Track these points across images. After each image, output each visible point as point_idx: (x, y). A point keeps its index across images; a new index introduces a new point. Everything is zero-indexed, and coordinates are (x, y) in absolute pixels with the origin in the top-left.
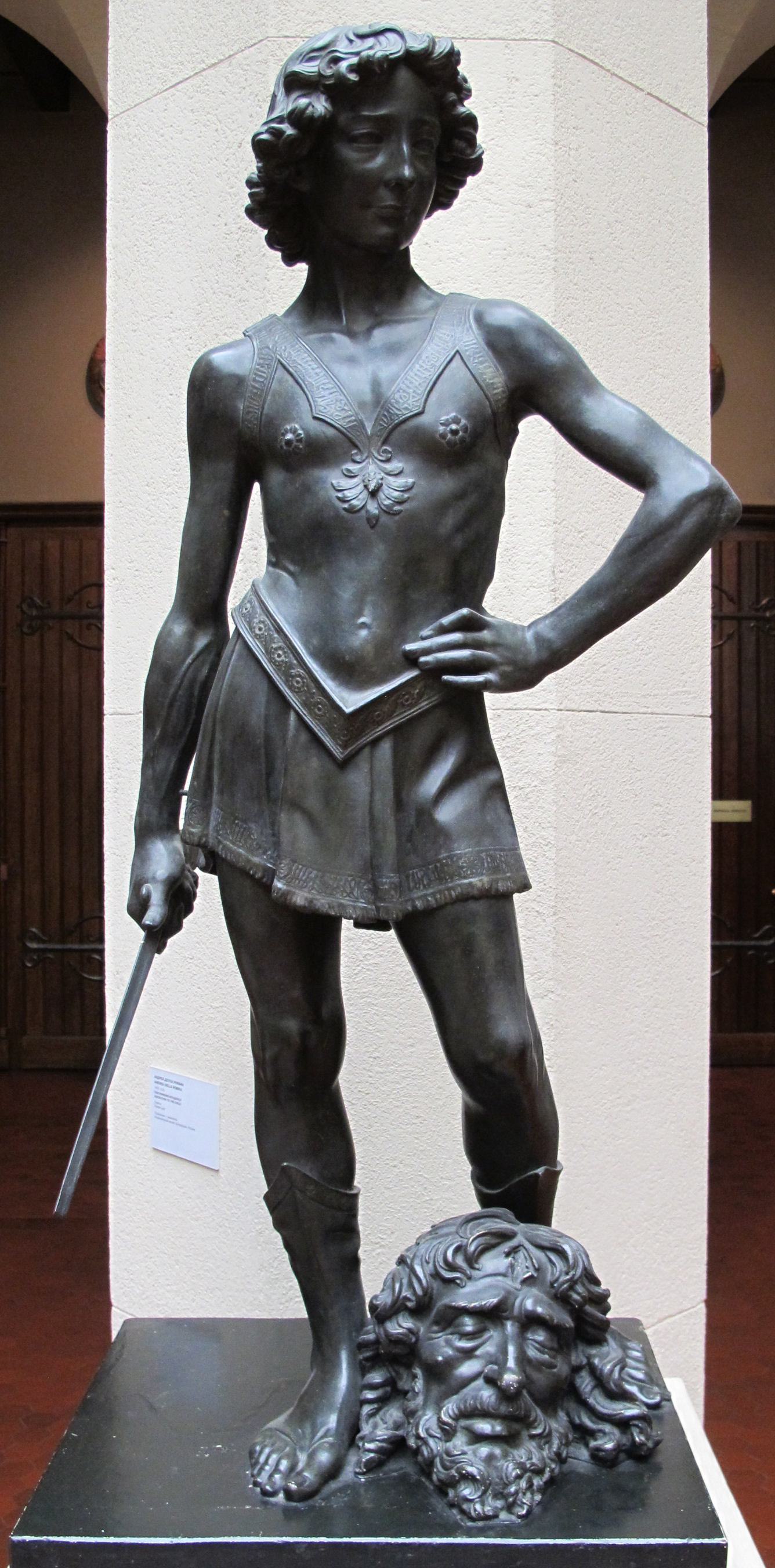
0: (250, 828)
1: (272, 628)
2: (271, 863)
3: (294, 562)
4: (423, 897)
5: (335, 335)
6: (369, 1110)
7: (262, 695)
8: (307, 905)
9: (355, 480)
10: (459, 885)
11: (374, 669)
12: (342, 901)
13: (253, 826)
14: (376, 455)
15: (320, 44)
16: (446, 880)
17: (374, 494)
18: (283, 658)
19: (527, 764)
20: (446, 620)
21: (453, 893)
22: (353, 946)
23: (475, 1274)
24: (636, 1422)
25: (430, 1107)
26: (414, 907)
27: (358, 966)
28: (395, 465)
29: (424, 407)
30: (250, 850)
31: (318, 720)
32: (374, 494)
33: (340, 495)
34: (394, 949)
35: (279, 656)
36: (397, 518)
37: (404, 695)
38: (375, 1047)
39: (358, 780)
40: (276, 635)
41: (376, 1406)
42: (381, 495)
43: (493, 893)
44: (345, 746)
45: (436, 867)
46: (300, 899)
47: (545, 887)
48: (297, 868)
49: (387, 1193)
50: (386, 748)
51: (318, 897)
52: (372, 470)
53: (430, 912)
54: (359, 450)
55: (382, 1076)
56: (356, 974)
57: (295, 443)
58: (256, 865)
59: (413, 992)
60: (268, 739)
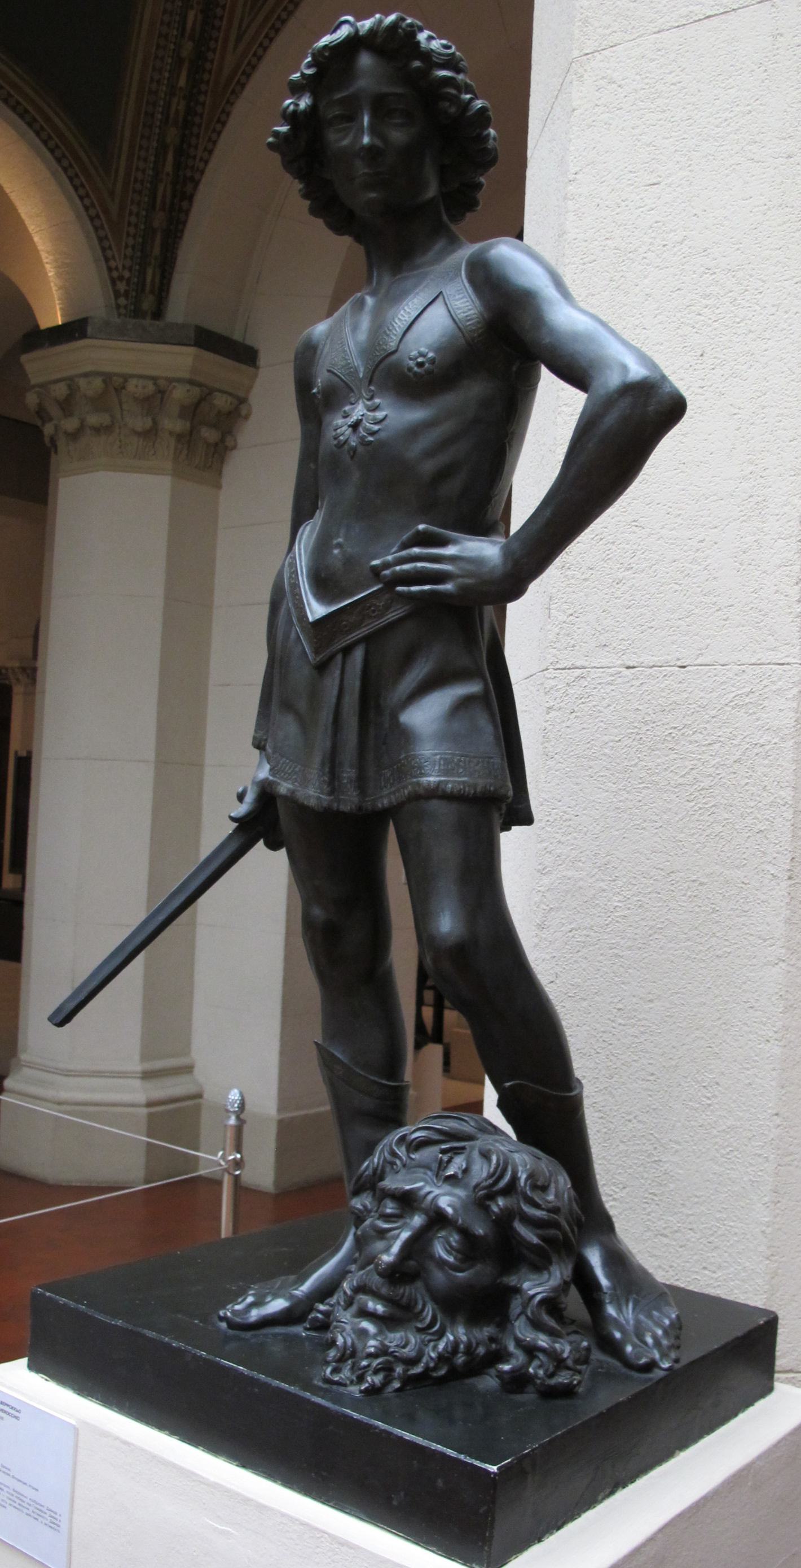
6: (611, 1061)
8: (289, 795)
19: (768, 721)
22: (605, 897)
25: (664, 1066)
27: (609, 917)
29: (398, 346)
34: (640, 903)
37: (370, 607)
38: (619, 998)
43: (440, 793)
47: (781, 849)
49: (622, 1147)
50: (359, 654)
51: (300, 789)
55: (625, 1028)
56: (607, 925)
59: (655, 947)
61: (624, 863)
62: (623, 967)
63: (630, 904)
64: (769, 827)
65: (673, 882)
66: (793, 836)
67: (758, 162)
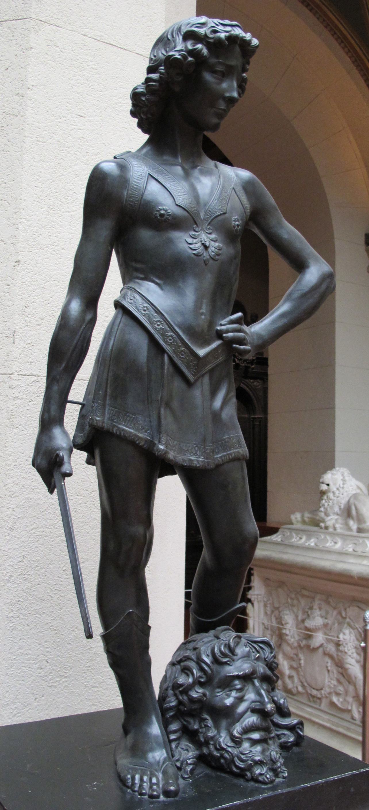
0: (137, 418)
2: (149, 437)
3: (159, 278)
6: (60, 600)
9: (197, 240)
11: (207, 337)
12: (191, 458)
13: (139, 417)
16: (228, 450)
18: (161, 326)
21: (231, 456)
22: (54, 508)
25: (91, 596)
27: (57, 519)
28: (213, 236)
30: (138, 430)
31: (181, 360)
34: (75, 509)
35: (158, 325)
36: (217, 262)
38: (64, 564)
40: (156, 314)
45: (222, 443)
49: (69, 647)
55: (68, 580)
56: (55, 524)
57: (166, 216)
58: (140, 438)
59: (85, 533)
65: (93, 497)
67: (136, 133)
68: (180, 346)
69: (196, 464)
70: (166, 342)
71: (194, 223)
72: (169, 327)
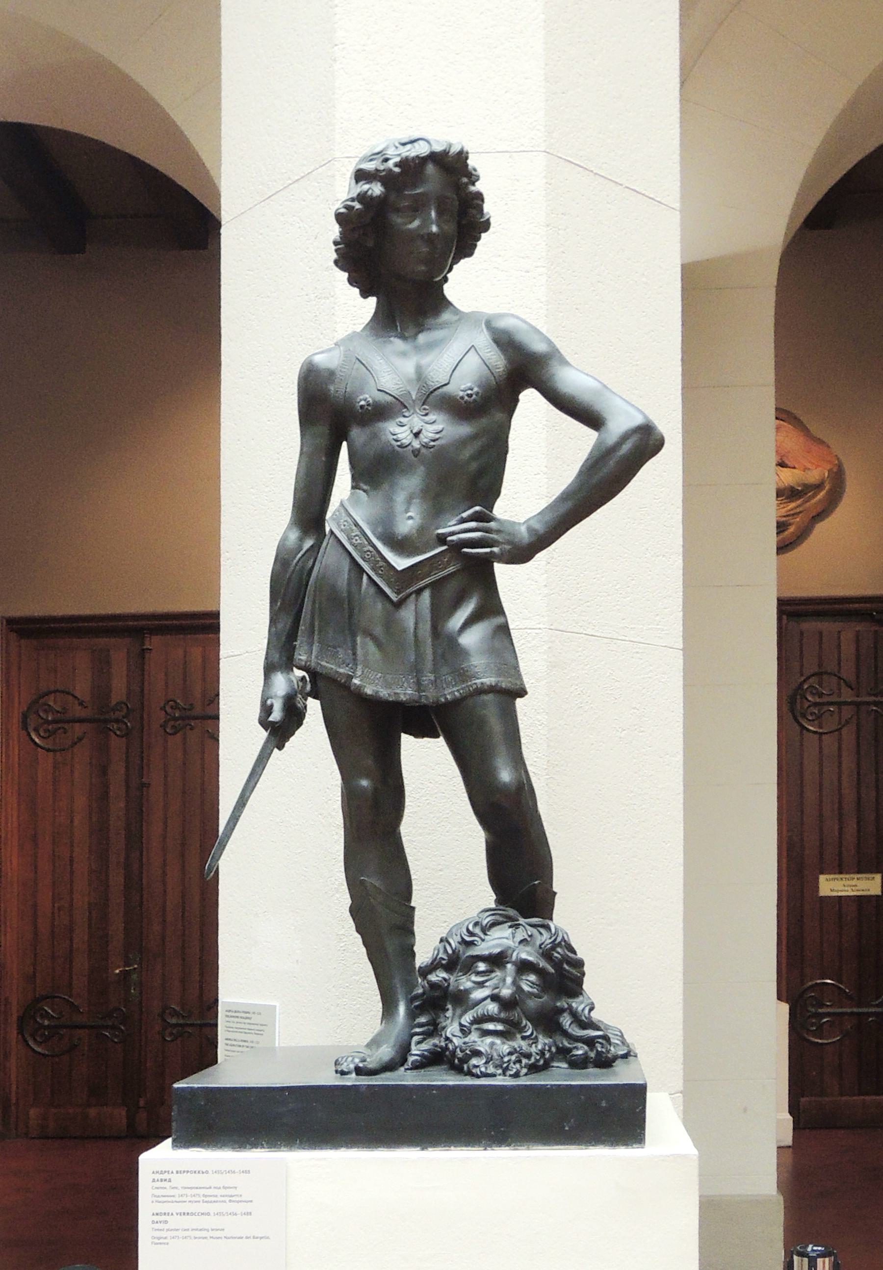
1: (352, 524)
4: (452, 692)
5: (392, 339)
7: (346, 564)
10: (475, 684)
14: (418, 411)
15: (377, 150)
17: (417, 435)
18: (359, 541)
20: (465, 515)
21: (471, 689)
23: (487, 938)
24: (600, 1040)
26: (446, 699)
28: (431, 417)
29: (450, 381)
31: (382, 578)
32: (417, 435)
33: (395, 437)
34: (428, 801)
35: (356, 540)
36: (432, 450)
39: (407, 615)
41: (422, 1037)
42: (421, 436)
43: (498, 689)
44: (398, 593)
46: (369, 691)
47: (540, 755)
48: (368, 671)
50: (426, 595)
51: (382, 690)
52: (416, 421)
53: (456, 703)
54: (408, 409)
57: (366, 407)
60: (349, 592)
61: (413, 774)
62: (416, 849)
63: (420, 802)
64: (530, 741)
65: (455, 784)
66: (548, 746)
68: (378, 561)
69: (403, 698)
70: (364, 559)
71: (402, 407)
72: (367, 541)
